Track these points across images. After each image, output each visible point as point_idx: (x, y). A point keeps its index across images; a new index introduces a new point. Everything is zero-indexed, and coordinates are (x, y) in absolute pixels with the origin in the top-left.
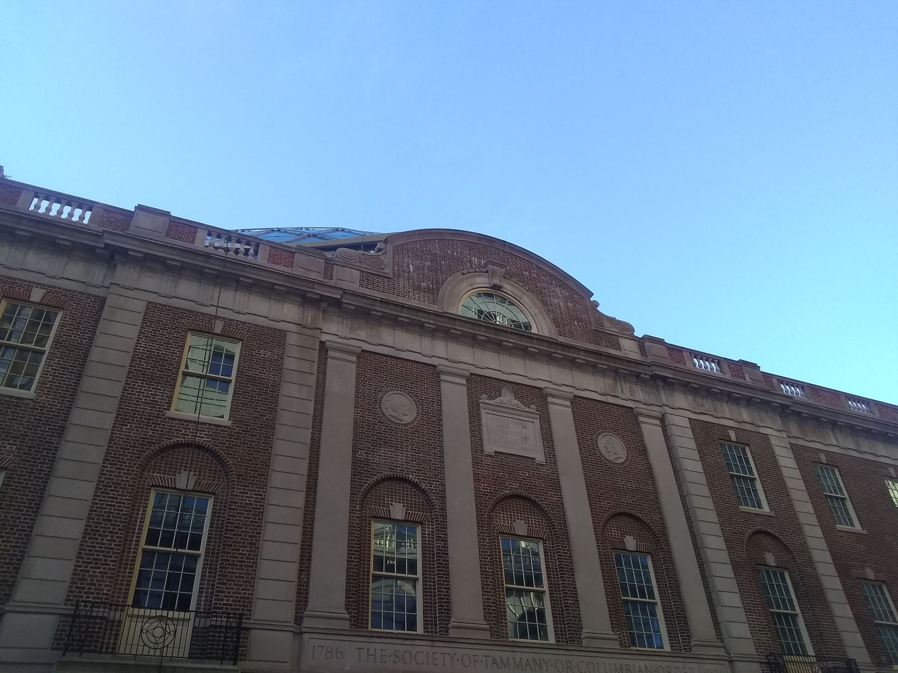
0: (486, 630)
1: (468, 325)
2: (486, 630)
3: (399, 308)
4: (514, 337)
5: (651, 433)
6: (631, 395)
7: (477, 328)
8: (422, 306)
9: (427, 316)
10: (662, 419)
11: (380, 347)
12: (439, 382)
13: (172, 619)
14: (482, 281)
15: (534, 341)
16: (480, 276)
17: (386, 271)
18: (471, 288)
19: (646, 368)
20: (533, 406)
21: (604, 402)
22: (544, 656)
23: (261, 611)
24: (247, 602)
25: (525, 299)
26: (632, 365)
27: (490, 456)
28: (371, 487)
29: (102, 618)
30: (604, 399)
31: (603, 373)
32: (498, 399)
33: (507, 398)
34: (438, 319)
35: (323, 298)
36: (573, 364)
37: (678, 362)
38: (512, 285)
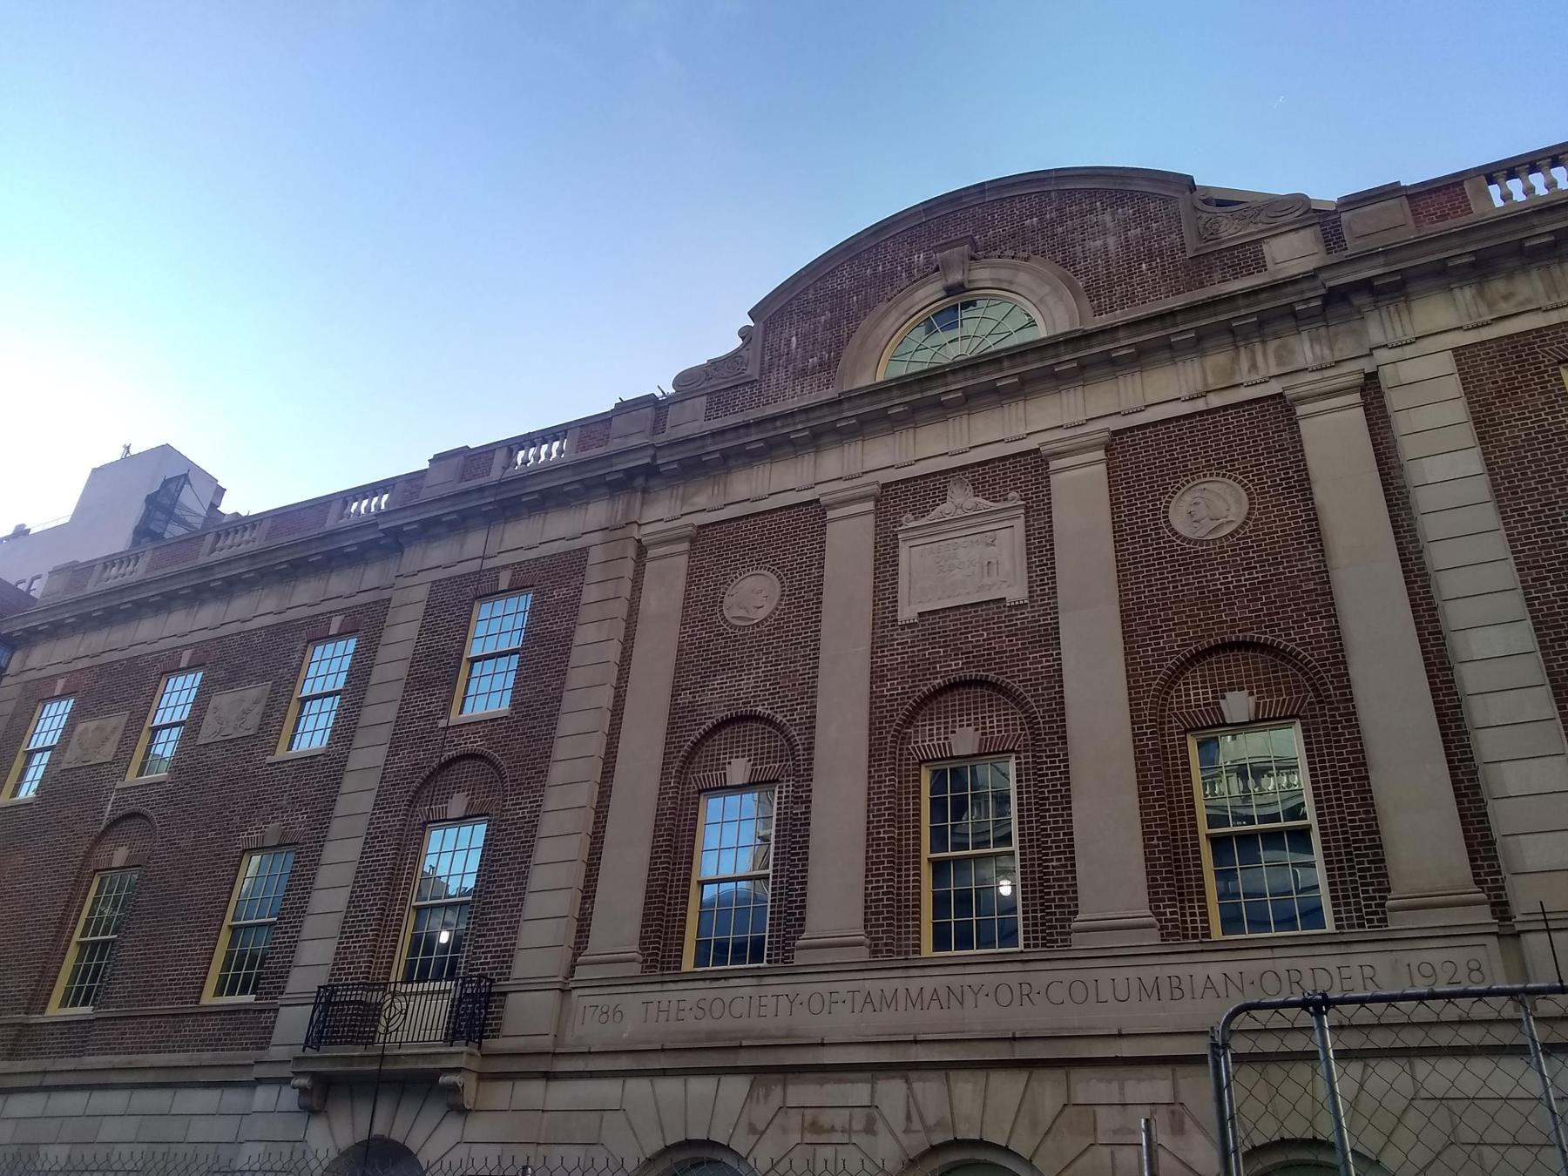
0: (1151, 926)
1: (866, 400)
2: (1151, 926)
3: (742, 431)
4: (960, 376)
5: (1333, 440)
6: (1280, 360)
7: (884, 396)
8: (807, 401)
9: (790, 420)
10: (1370, 386)
11: (973, 452)
12: (1293, 424)
13: (405, 994)
14: (929, 293)
15: (1006, 364)
16: (924, 285)
17: (747, 372)
18: (904, 318)
19: (1305, 285)
20: (1013, 494)
21: (1201, 413)
22: (968, 980)
23: (524, 966)
24: (506, 957)
25: (1023, 277)
26: (1263, 296)
27: (910, 626)
28: (696, 746)
29: (356, 1002)
30: (1200, 405)
31: (1199, 344)
32: (934, 515)
33: (960, 499)
34: (812, 415)
35: (631, 474)
36: (1113, 365)
37: (1443, 217)
38: (993, 266)
